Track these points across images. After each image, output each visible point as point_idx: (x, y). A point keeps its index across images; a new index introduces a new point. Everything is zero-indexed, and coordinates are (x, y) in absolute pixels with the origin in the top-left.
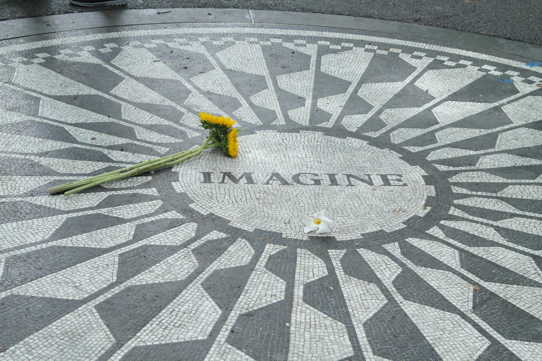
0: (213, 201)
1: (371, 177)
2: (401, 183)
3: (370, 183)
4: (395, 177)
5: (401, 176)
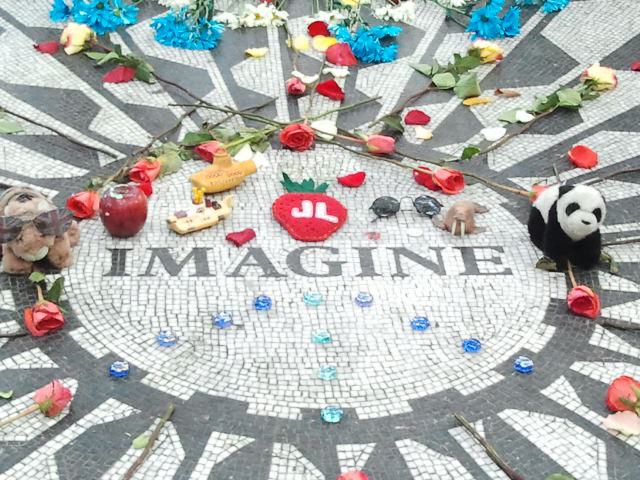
0: (120, 321)
1: (443, 253)
2: (500, 268)
3: (439, 269)
4: (488, 254)
5: (500, 250)
